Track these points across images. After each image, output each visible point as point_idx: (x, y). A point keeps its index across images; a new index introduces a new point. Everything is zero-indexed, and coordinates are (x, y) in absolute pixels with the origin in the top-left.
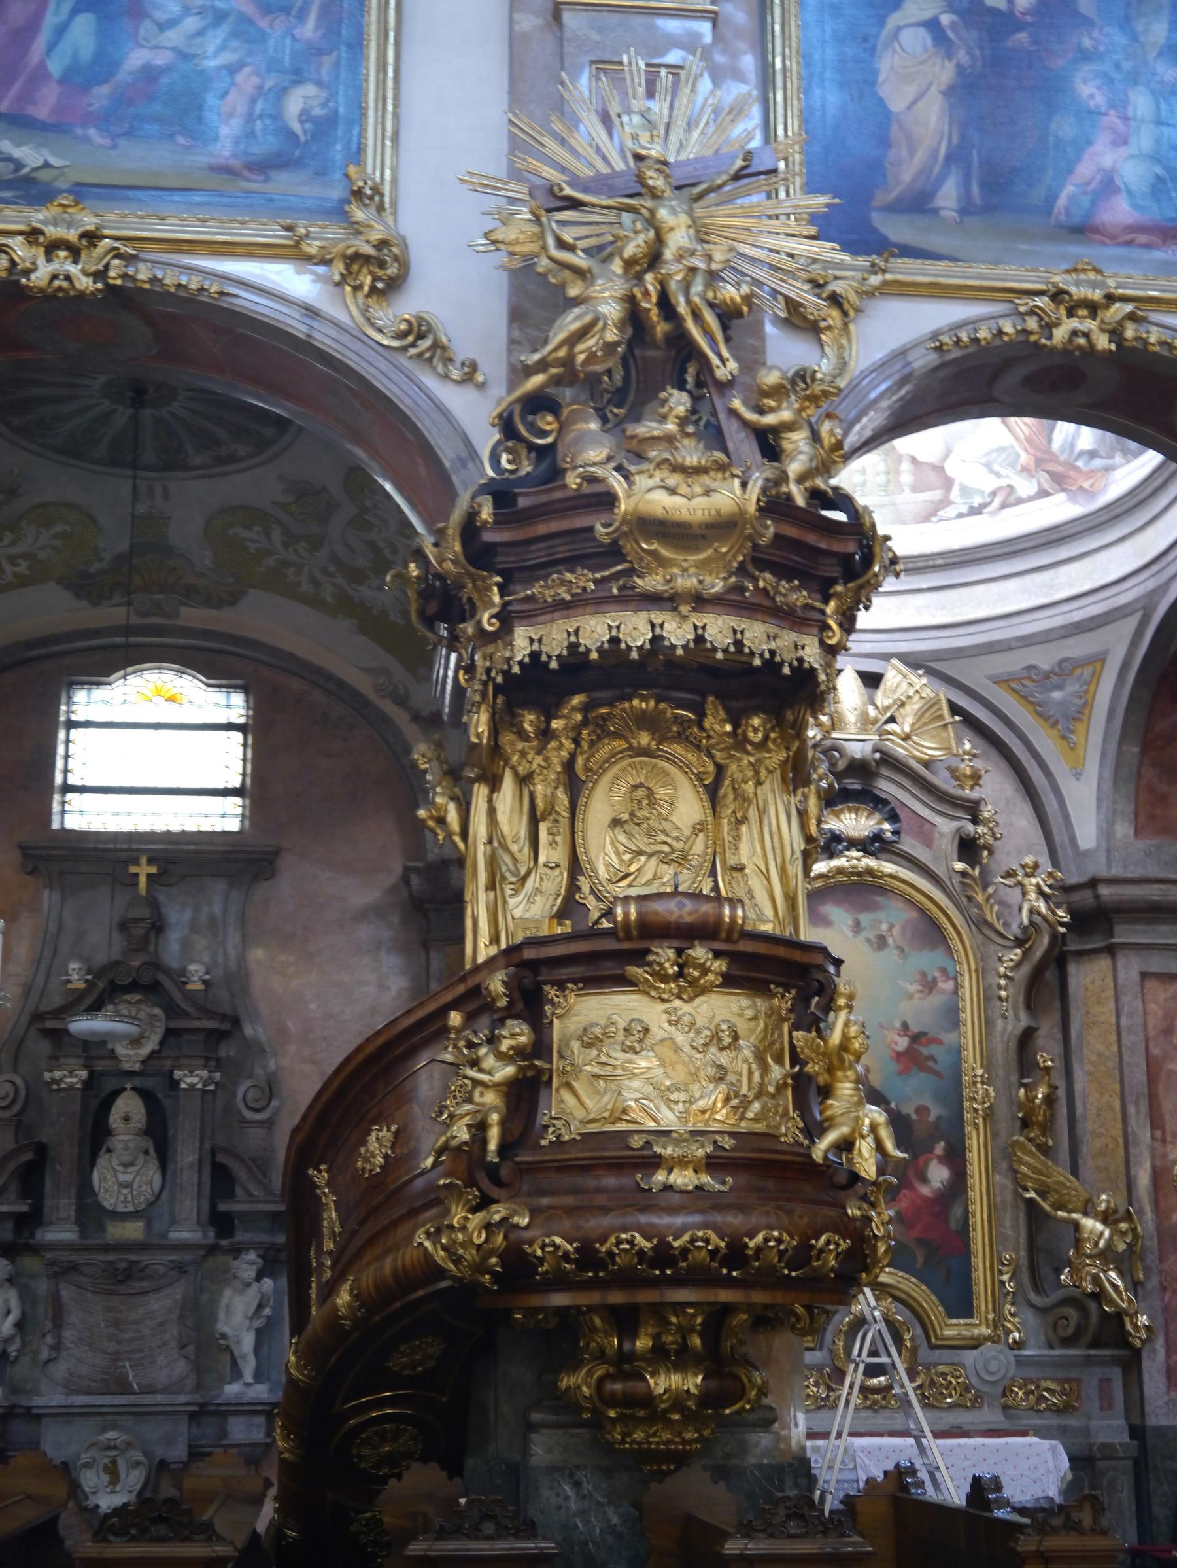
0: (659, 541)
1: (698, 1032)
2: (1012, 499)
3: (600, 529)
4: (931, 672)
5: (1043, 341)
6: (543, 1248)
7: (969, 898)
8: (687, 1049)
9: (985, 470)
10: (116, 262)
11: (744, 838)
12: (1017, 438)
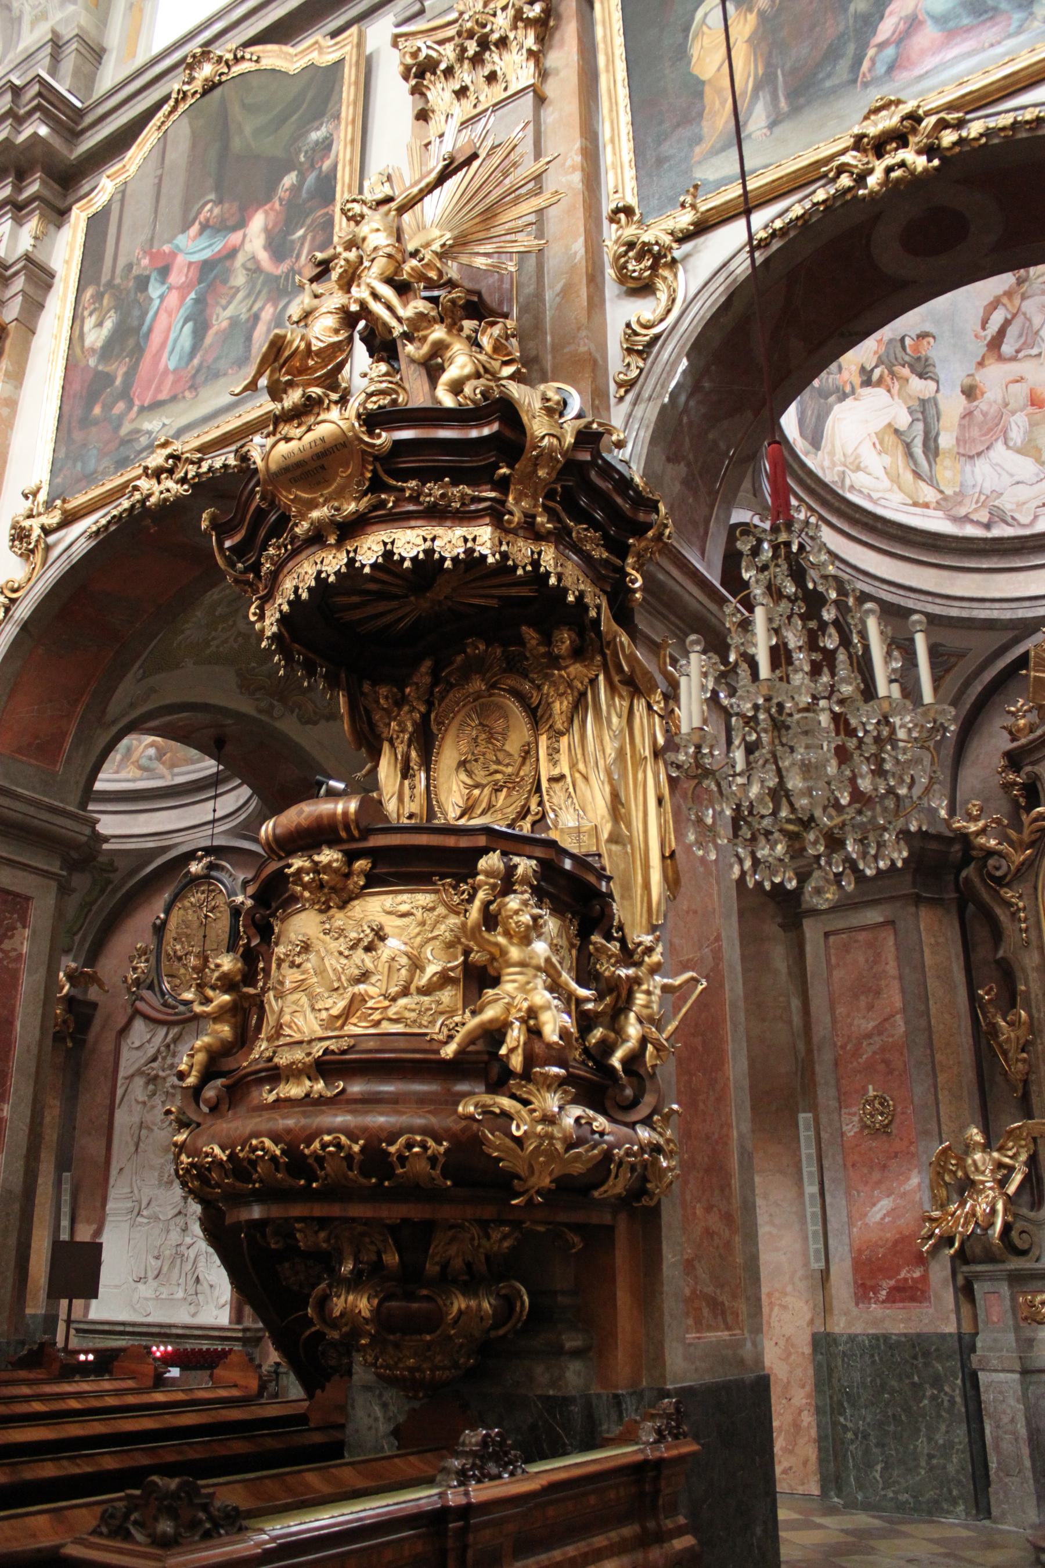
5: (861, 192)
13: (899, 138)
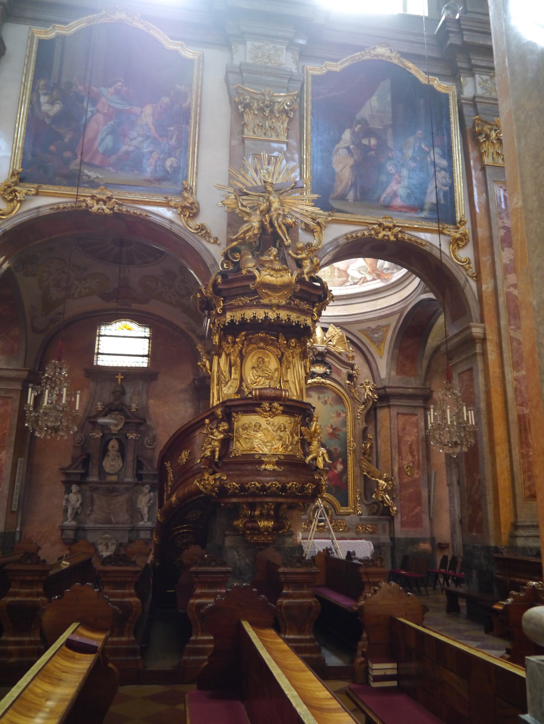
0: (268, 290)
1: (275, 427)
2: (365, 281)
3: (251, 285)
4: (341, 328)
6: (230, 486)
7: (350, 391)
8: (272, 431)
9: (358, 272)
10: (117, 205)
11: (289, 373)
12: (367, 263)
13: (390, 229)
